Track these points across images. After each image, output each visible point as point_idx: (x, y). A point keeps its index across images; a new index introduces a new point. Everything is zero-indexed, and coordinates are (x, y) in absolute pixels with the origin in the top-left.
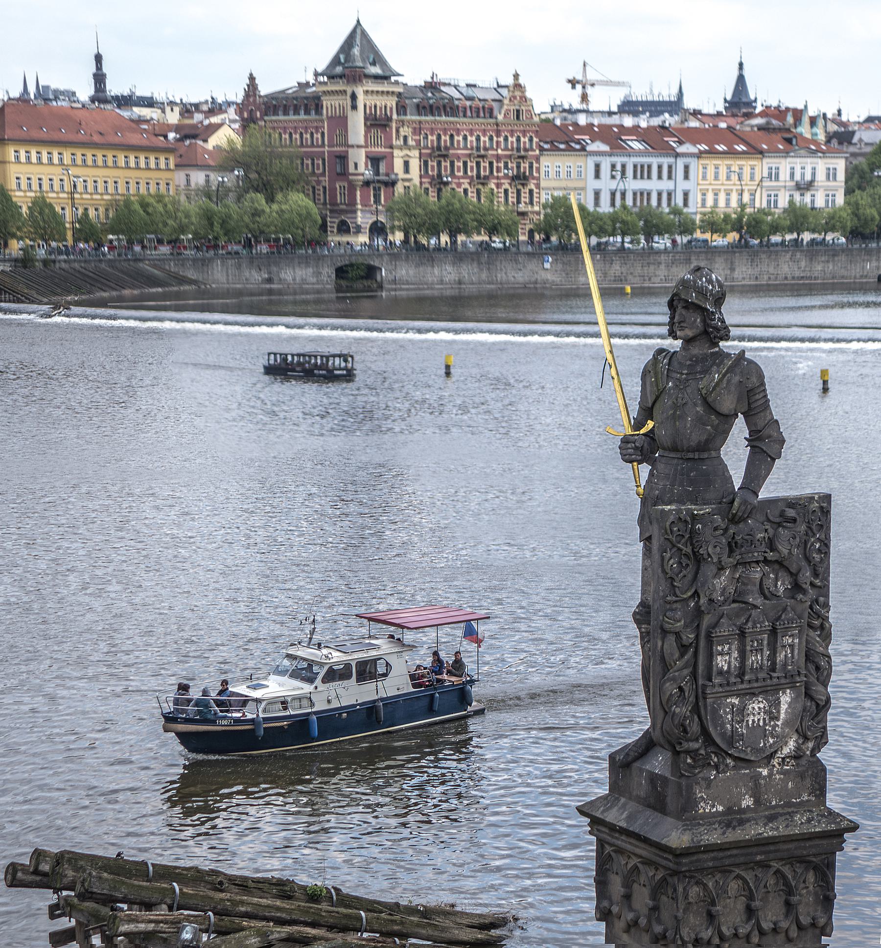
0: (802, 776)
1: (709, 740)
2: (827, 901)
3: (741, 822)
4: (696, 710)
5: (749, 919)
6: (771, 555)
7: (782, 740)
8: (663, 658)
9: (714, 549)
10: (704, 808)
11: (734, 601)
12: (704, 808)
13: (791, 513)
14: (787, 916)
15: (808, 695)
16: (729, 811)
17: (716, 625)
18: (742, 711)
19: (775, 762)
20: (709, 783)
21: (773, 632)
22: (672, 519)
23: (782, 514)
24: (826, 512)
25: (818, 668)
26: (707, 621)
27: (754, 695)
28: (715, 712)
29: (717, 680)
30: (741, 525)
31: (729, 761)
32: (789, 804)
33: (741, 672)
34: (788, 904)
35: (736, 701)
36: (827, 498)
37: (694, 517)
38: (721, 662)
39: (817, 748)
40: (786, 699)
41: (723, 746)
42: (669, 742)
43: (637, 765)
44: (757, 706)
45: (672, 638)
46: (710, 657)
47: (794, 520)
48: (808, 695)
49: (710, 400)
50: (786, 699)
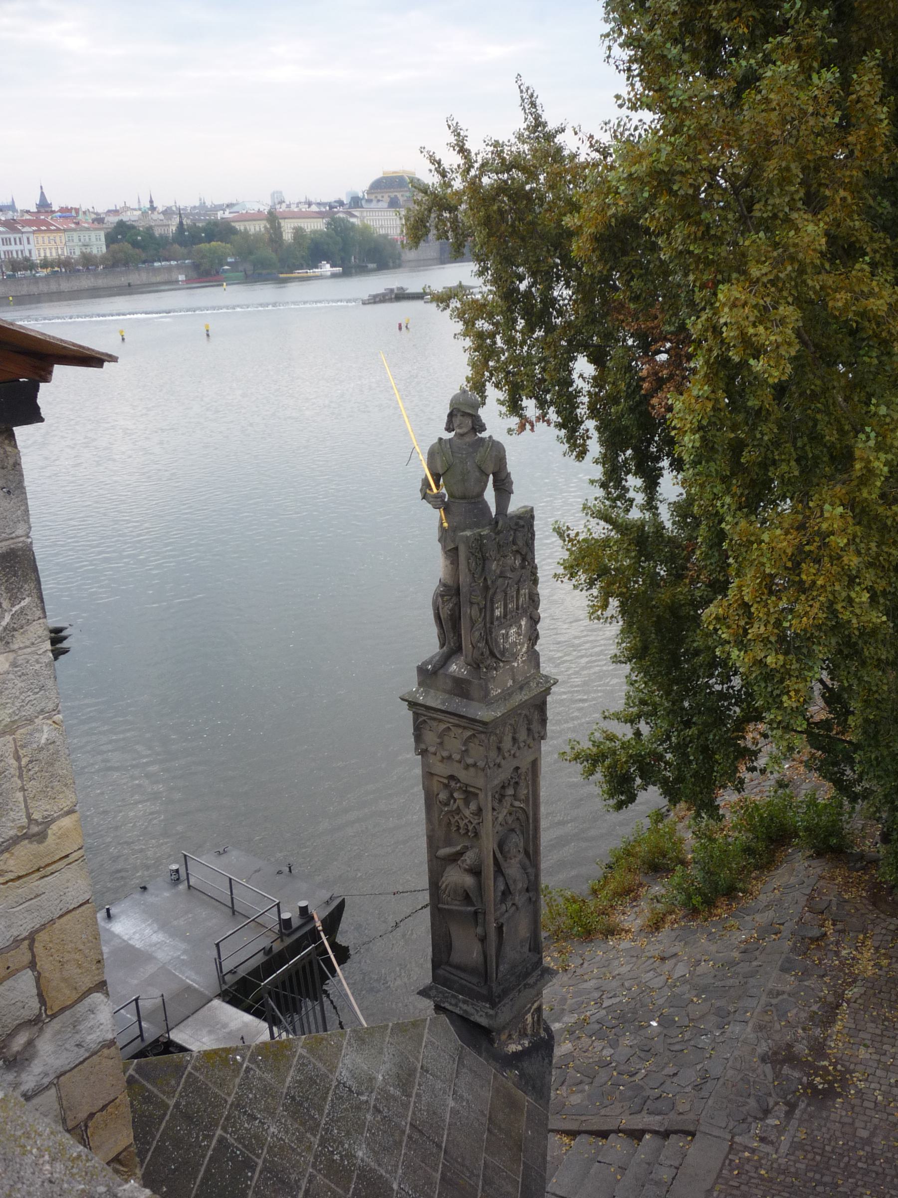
0: (530, 662)
1: (492, 654)
2: (543, 721)
3: (510, 695)
4: (487, 643)
5: (514, 744)
6: (514, 548)
7: (522, 644)
8: (471, 617)
9: (492, 553)
10: (494, 693)
11: (500, 577)
12: (494, 693)
13: (522, 523)
14: (528, 735)
15: (531, 618)
16: (503, 691)
17: (495, 593)
18: (506, 636)
19: (519, 658)
20: (493, 678)
21: (518, 591)
22: (472, 540)
23: (517, 524)
24: (532, 517)
25: (533, 601)
26: (491, 592)
27: (511, 625)
28: (496, 640)
29: (496, 623)
30: (501, 535)
31: (501, 664)
32: (526, 678)
33: (505, 616)
34: (529, 730)
35: (504, 631)
36: (532, 509)
37: (480, 535)
38: (497, 613)
39: (534, 644)
40: (523, 623)
41: (498, 656)
42: (476, 663)
43: (441, 671)
44: (513, 630)
45: (476, 606)
46: (493, 611)
47: (523, 526)
48: (531, 618)
49: (483, 468)
50: (523, 623)
